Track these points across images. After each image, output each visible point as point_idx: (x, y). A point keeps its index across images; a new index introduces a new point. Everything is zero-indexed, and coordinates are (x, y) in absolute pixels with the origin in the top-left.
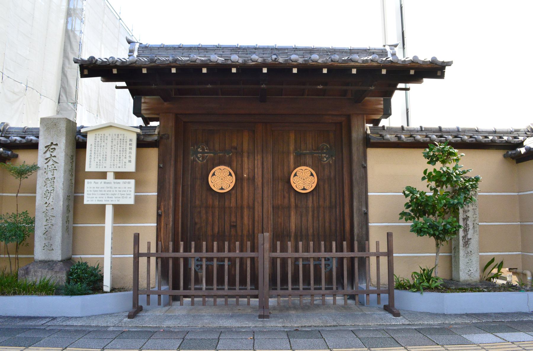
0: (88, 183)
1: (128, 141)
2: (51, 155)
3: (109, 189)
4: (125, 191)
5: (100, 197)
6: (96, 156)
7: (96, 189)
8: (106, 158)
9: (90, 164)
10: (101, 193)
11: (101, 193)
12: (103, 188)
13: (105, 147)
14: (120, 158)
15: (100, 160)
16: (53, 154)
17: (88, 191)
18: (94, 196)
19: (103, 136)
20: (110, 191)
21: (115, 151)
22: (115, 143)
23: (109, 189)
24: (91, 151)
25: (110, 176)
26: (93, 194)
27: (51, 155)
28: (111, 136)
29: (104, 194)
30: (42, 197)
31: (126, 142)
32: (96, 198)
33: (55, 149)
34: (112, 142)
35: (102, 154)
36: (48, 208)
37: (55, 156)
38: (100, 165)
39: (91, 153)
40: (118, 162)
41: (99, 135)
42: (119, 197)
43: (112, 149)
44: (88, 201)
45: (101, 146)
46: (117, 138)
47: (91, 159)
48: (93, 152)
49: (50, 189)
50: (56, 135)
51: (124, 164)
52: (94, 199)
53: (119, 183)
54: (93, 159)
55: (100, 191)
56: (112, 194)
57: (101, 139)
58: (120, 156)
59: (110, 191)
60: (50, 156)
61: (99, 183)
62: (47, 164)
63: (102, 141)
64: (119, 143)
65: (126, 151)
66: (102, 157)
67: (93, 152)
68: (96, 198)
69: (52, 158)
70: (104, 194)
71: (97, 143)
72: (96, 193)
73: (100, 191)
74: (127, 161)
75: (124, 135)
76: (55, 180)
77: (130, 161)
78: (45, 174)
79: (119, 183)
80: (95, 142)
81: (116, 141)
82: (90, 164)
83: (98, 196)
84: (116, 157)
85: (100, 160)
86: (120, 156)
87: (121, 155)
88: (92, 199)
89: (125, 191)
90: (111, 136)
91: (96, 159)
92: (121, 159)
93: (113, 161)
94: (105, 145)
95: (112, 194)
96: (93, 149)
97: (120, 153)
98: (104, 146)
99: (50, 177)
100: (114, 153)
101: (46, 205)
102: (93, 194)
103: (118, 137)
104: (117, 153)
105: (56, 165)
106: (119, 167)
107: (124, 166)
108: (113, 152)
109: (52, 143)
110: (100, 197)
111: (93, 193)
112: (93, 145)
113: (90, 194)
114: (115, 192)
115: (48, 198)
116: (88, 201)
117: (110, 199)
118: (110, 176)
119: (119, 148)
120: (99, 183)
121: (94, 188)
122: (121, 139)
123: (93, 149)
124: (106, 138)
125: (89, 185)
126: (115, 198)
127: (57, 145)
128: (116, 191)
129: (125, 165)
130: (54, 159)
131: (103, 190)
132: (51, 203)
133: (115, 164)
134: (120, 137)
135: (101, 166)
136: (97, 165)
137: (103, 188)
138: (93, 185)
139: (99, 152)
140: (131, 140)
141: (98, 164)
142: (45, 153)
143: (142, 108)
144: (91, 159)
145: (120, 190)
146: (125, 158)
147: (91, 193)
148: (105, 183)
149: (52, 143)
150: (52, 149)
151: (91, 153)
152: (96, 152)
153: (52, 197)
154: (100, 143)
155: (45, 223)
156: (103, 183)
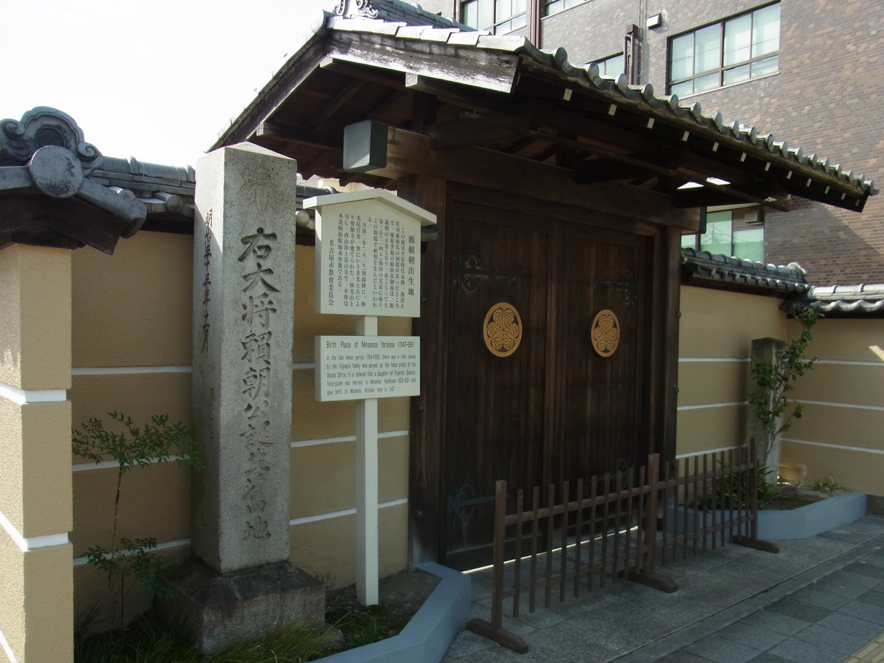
0: (328, 345)
1: (407, 240)
2: (259, 265)
3: (373, 361)
4: (404, 365)
5: (355, 383)
6: (343, 275)
7: (345, 362)
8: (364, 280)
9: (331, 295)
10: (357, 370)
11: (357, 370)
12: (362, 358)
13: (361, 251)
14: (392, 282)
15: (352, 285)
16: (266, 264)
17: (328, 367)
18: (343, 380)
19: (355, 220)
20: (375, 366)
21: (381, 263)
22: (381, 242)
23: (373, 361)
24: (331, 258)
25: (371, 326)
26: (340, 375)
27: (259, 265)
28: (373, 223)
29: (364, 374)
30: (237, 392)
31: (403, 242)
32: (347, 383)
33: (268, 248)
34: (375, 239)
35: (355, 270)
36: (253, 422)
37: (270, 271)
38: (352, 298)
39: (331, 265)
40: (389, 291)
41: (347, 216)
42: (394, 381)
43: (375, 257)
44: (330, 393)
45: (352, 248)
46: (384, 231)
47: (331, 280)
48: (336, 262)
49: (259, 366)
50: (270, 209)
51: (400, 297)
52: (343, 387)
53: (392, 345)
54: (336, 283)
55: (356, 366)
56: (379, 374)
57: (352, 230)
58: (392, 276)
59: (375, 366)
60: (254, 268)
61: (352, 345)
62: (248, 293)
63: (355, 234)
64: (390, 244)
65: (403, 265)
66: (355, 276)
67: (336, 262)
68: (347, 383)
69: (261, 274)
70: (364, 374)
71: (343, 238)
72: (346, 371)
73: (356, 366)
74: (406, 292)
75: (398, 224)
76: (271, 342)
77: (411, 292)
78: (245, 322)
79: (392, 345)
80: (340, 234)
81: (384, 237)
82: (331, 295)
83: (351, 379)
84: (384, 278)
85: (352, 285)
86: (392, 276)
87: (395, 274)
88: (338, 388)
89: (404, 365)
90: (373, 223)
91: (343, 282)
92: (395, 285)
93: (378, 290)
94: (361, 246)
95: (379, 374)
96: (336, 256)
97: (392, 270)
98: (358, 248)
99: (259, 331)
100: (381, 269)
101: (250, 413)
102: (340, 375)
103: (387, 228)
104: (386, 269)
105: (272, 295)
106: (392, 305)
107: (400, 304)
108: (378, 266)
109: (260, 231)
110: (355, 383)
111: (341, 371)
112: (336, 243)
113: (333, 376)
114: (384, 369)
115: (253, 392)
116: (330, 393)
117: (375, 386)
118: (371, 326)
119: (389, 255)
120: (352, 345)
121: (341, 358)
122: (392, 235)
123: (336, 256)
124: (362, 227)
125: (330, 348)
126: (387, 381)
127: (273, 236)
128: (387, 365)
129: (402, 300)
130: (268, 278)
131: (361, 362)
132: (263, 408)
133: (384, 296)
134: (392, 229)
135: (355, 302)
136: (346, 296)
137: (362, 358)
138: (340, 351)
139: (349, 263)
140: (412, 239)
141: (349, 294)
142: (241, 259)
143: (389, 155)
144: (331, 280)
145: (394, 361)
146: (403, 283)
147: (335, 371)
148: (364, 345)
149: (260, 231)
150: (260, 248)
151: (331, 265)
152: (343, 263)
153: (264, 389)
154: (350, 239)
155: (247, 466)
156: (360, 345)
